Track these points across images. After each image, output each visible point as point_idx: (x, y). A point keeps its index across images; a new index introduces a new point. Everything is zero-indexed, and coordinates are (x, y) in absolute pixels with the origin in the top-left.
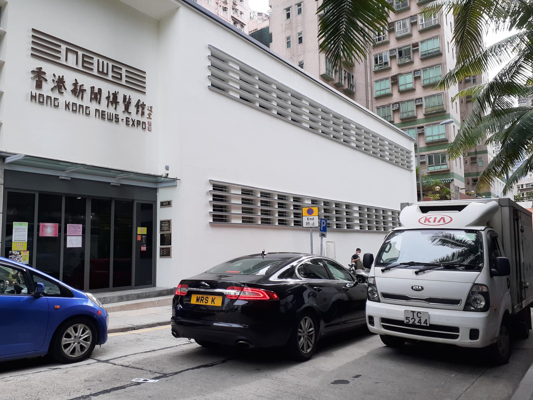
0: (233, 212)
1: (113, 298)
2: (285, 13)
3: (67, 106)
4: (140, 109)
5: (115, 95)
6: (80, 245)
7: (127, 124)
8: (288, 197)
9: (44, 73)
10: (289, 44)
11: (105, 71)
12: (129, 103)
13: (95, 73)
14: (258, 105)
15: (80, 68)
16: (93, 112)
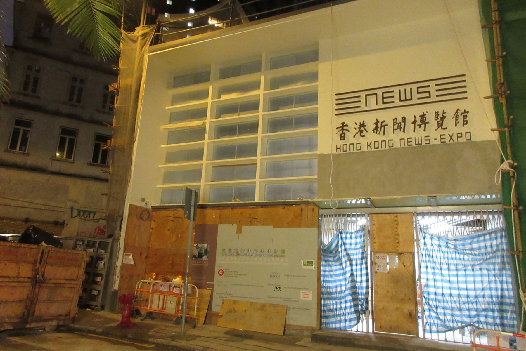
4: (461, 119)
5: (423, 117)
9: (347, 126)
11: (408, 97)
12: (443, 118)
13: (398, 103)
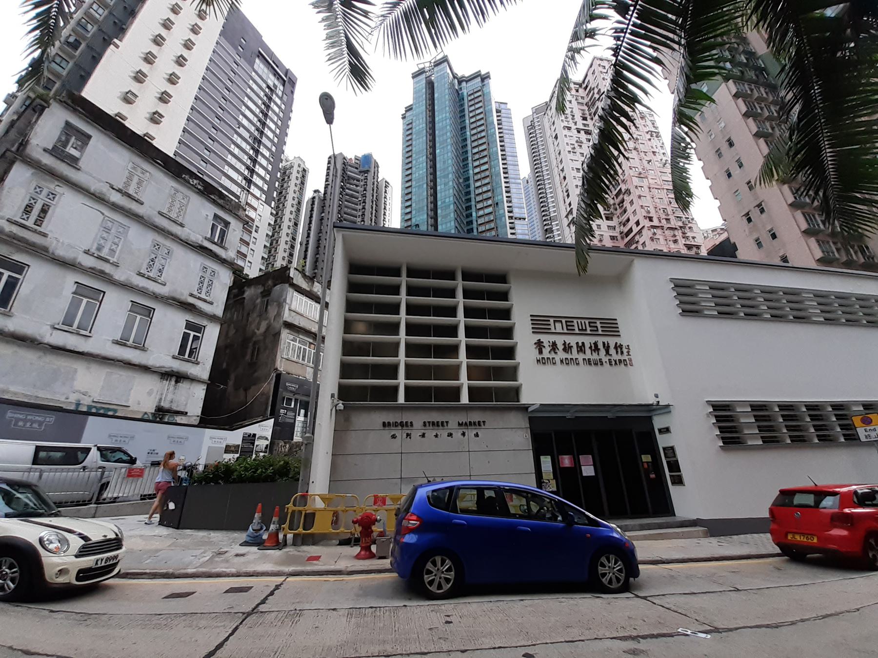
0: (746, 432)
1: (635, 525)
2: (745, 219)
3: (562, 361)
5: (596, 344)
6: (593, 474)
7: (611, 364)
8: (822, 406)
10: (759, 244)
12: (608, 347)
13: (577, 331)
14: (742, 315)
15: (566, 331)
16: (581, 362)
